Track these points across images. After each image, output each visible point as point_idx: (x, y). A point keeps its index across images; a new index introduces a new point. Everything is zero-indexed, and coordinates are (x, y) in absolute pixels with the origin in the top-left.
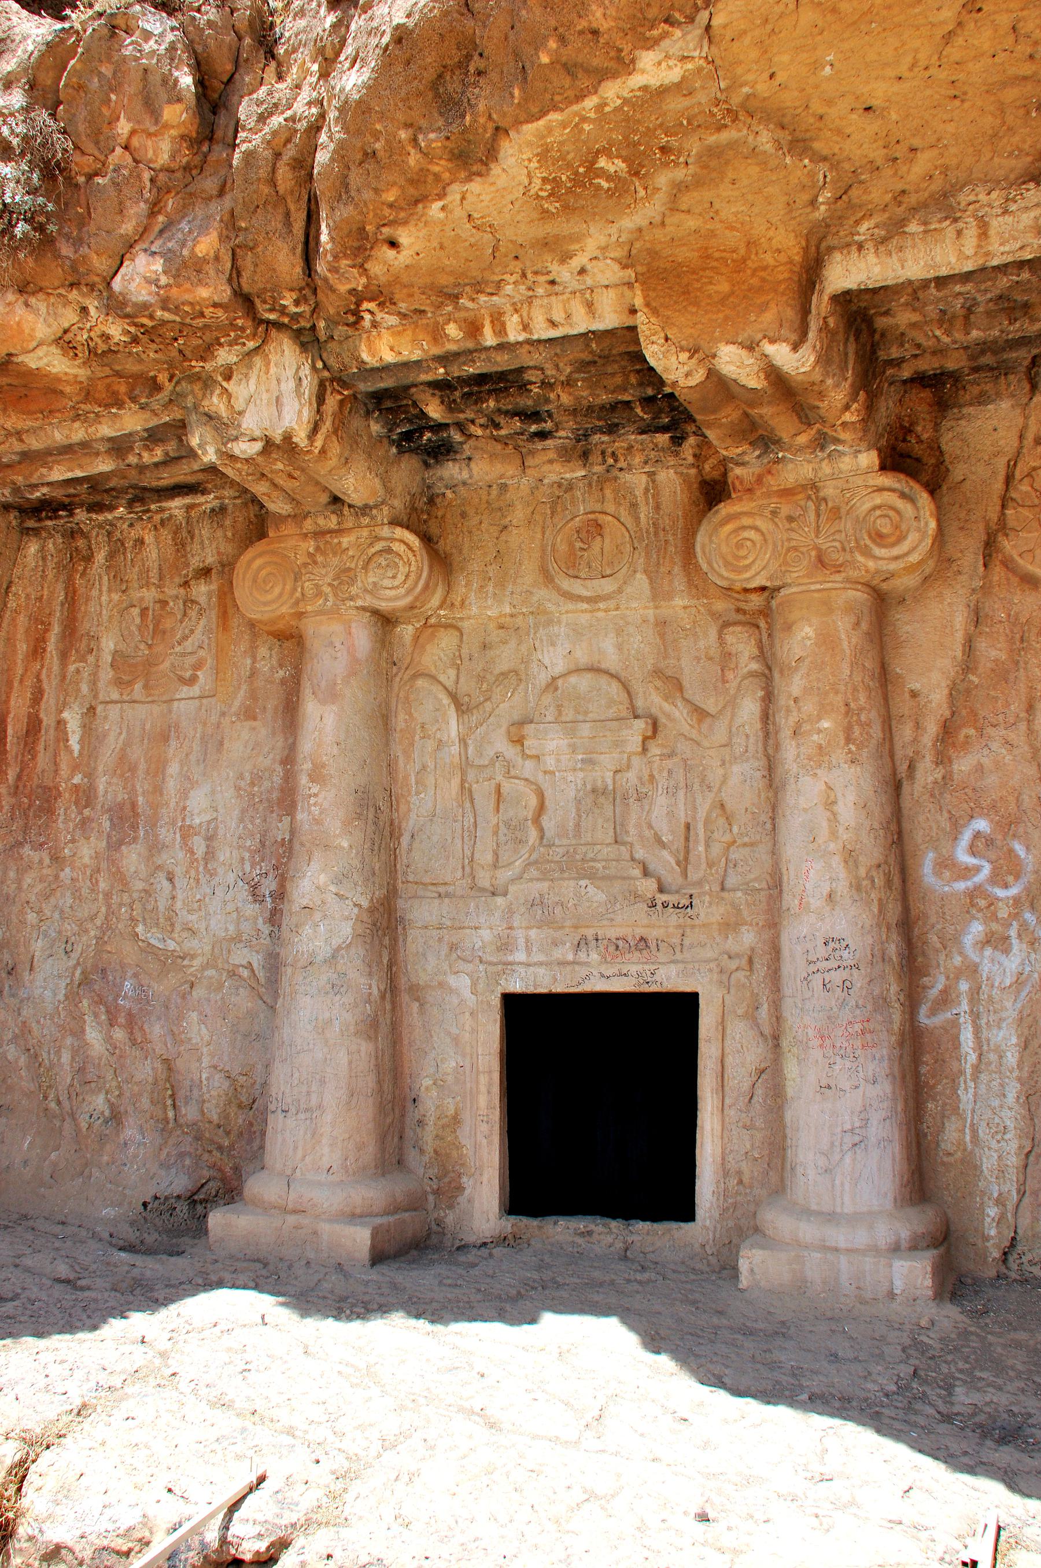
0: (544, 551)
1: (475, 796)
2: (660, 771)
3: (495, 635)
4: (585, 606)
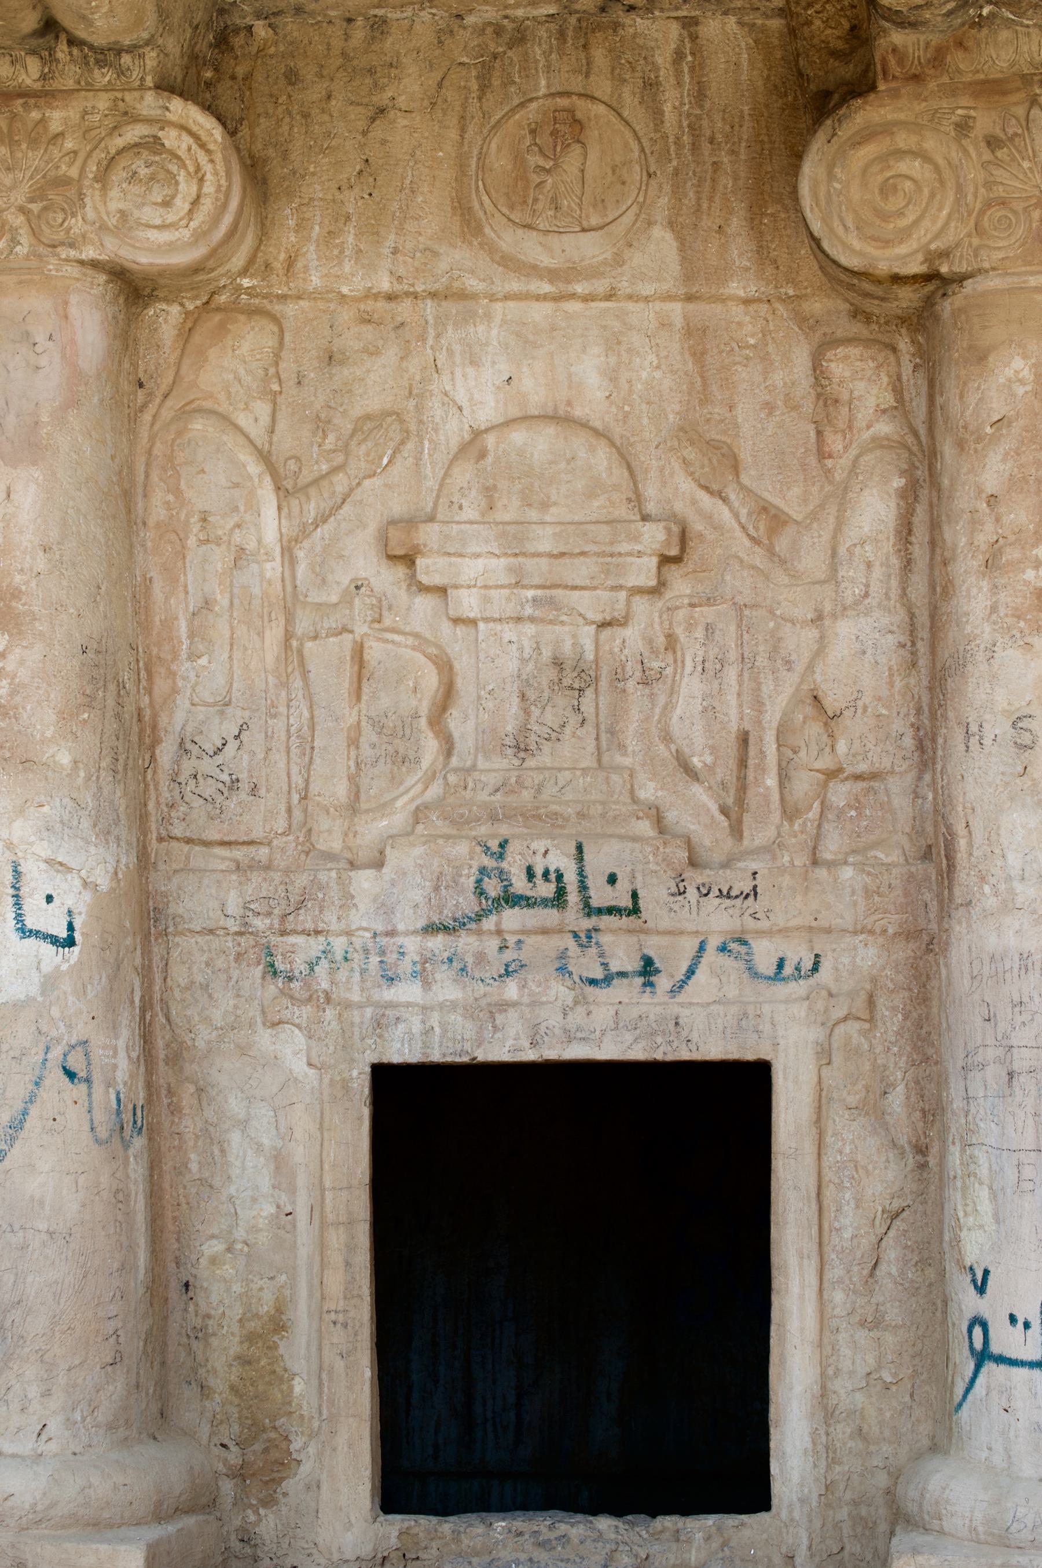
0: (461, 165)
1: (311, 667)
2: (690, 627)
3: (352, 338)
4: (546, 288)
